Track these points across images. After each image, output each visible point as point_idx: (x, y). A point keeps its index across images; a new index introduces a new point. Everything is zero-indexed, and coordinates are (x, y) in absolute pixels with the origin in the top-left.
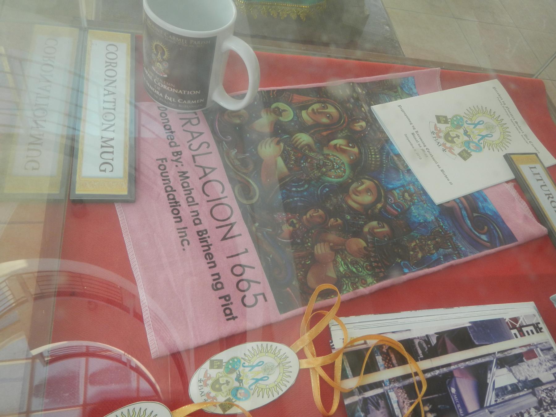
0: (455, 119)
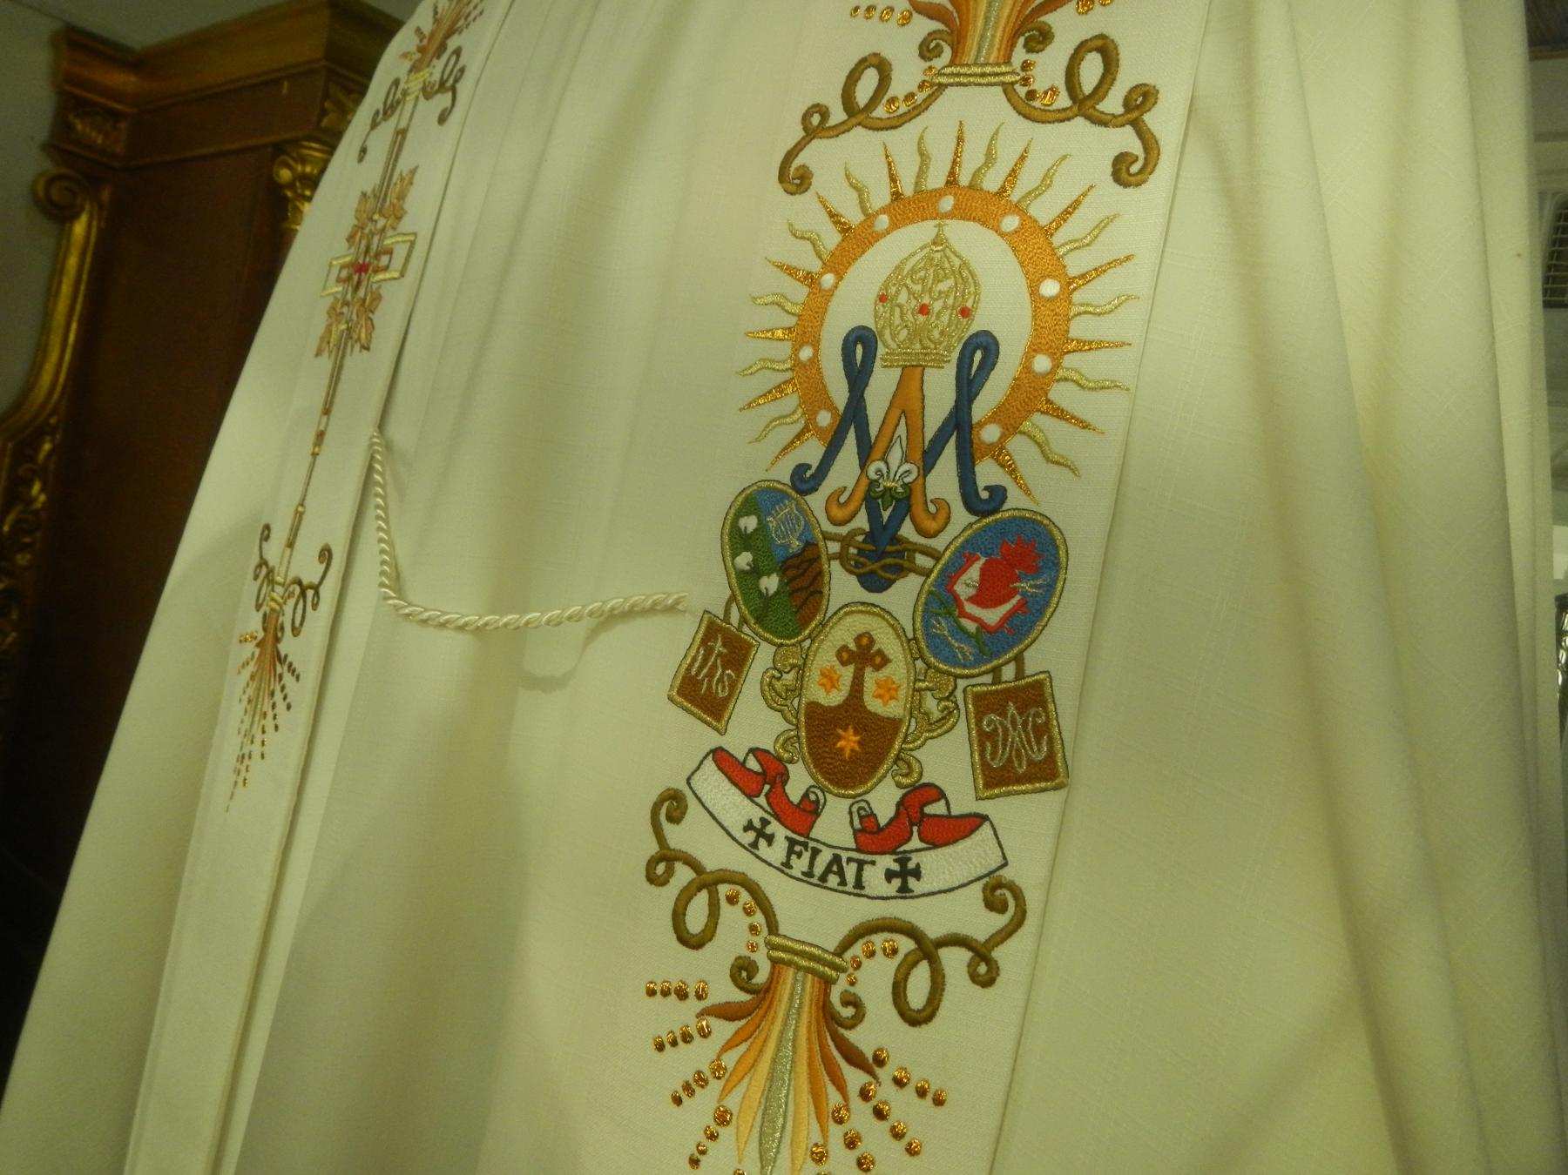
0: (744, 560)
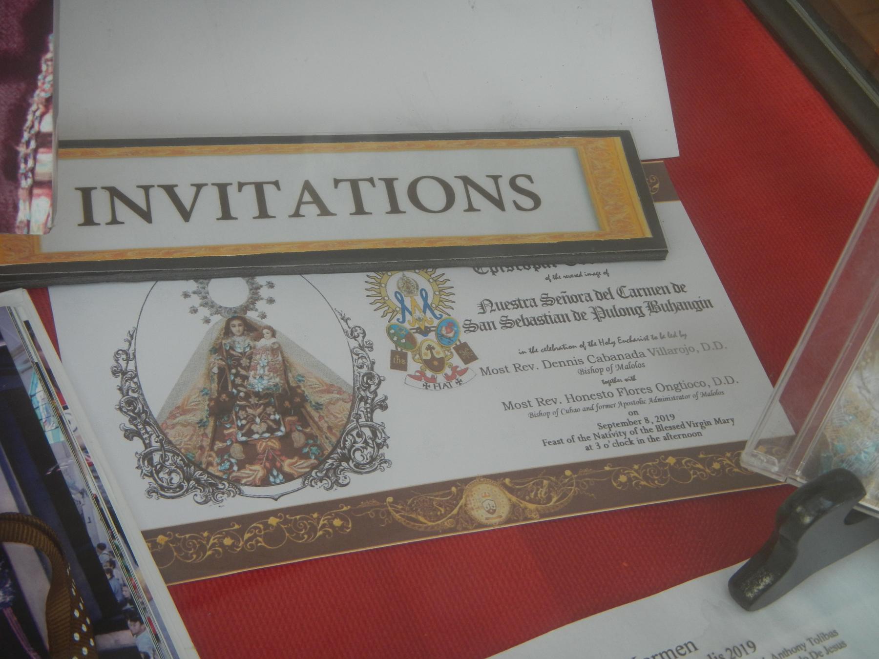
0: (395, 339)
